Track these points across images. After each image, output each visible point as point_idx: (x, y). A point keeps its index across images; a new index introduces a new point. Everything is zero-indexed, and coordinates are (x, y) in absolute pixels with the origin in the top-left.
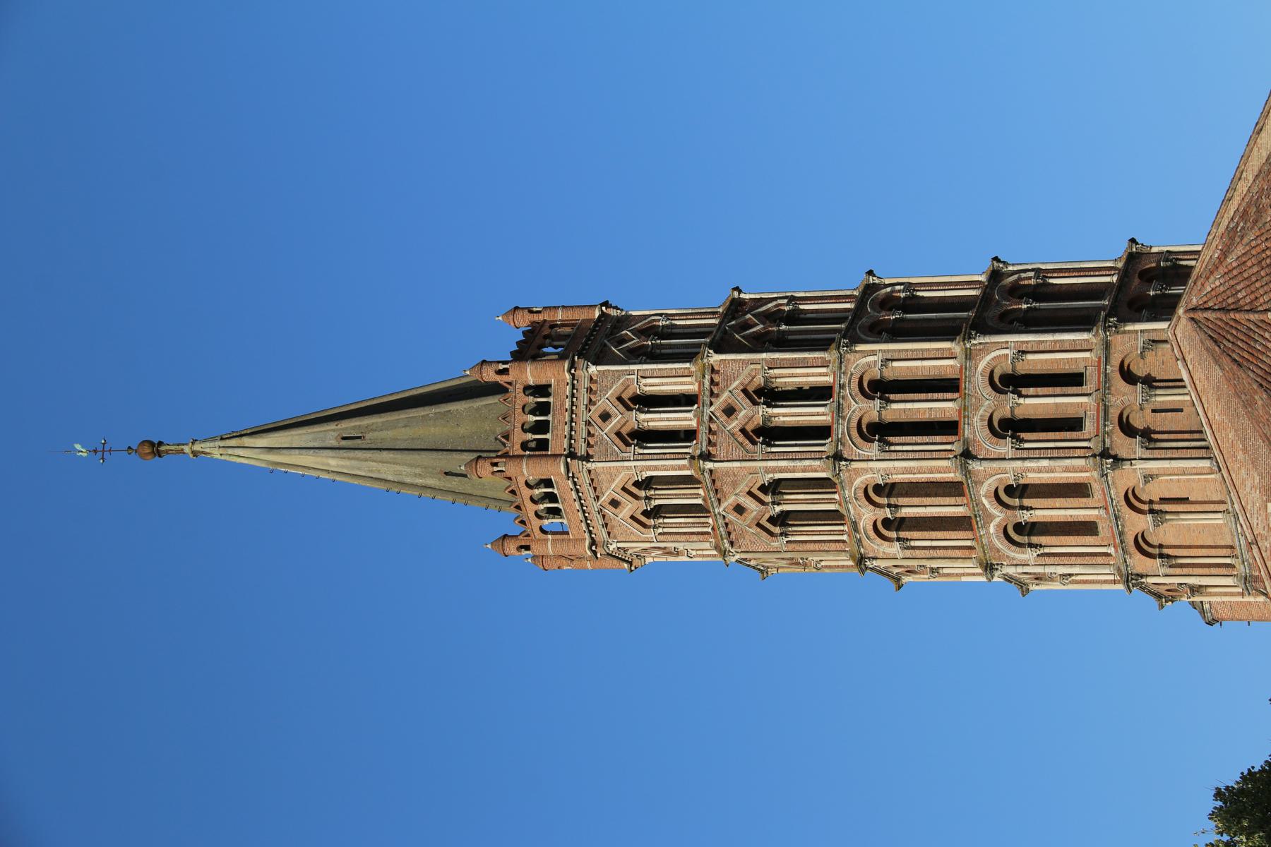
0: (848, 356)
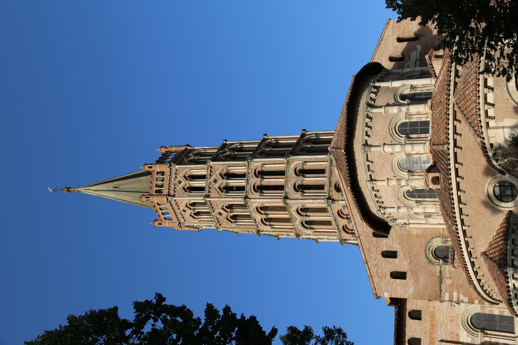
0: (251, 163)
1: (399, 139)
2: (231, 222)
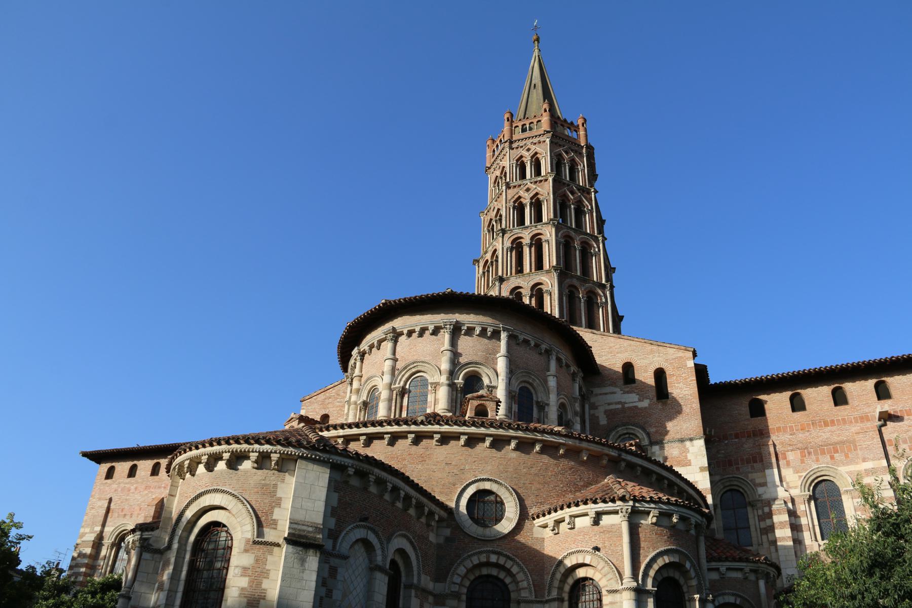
0: (550, 226)
1: (401, 380)
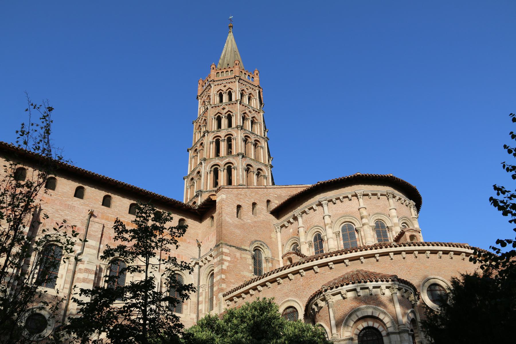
2: (215, 115)
